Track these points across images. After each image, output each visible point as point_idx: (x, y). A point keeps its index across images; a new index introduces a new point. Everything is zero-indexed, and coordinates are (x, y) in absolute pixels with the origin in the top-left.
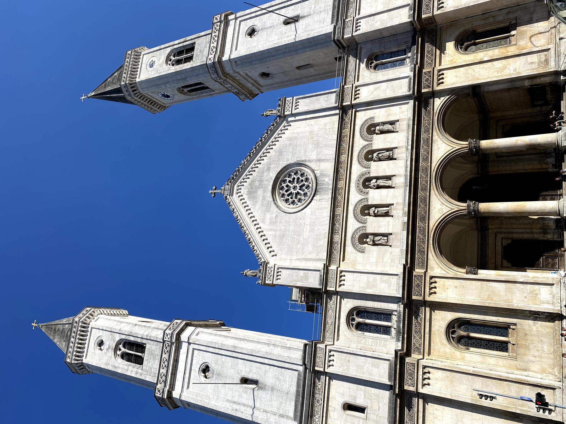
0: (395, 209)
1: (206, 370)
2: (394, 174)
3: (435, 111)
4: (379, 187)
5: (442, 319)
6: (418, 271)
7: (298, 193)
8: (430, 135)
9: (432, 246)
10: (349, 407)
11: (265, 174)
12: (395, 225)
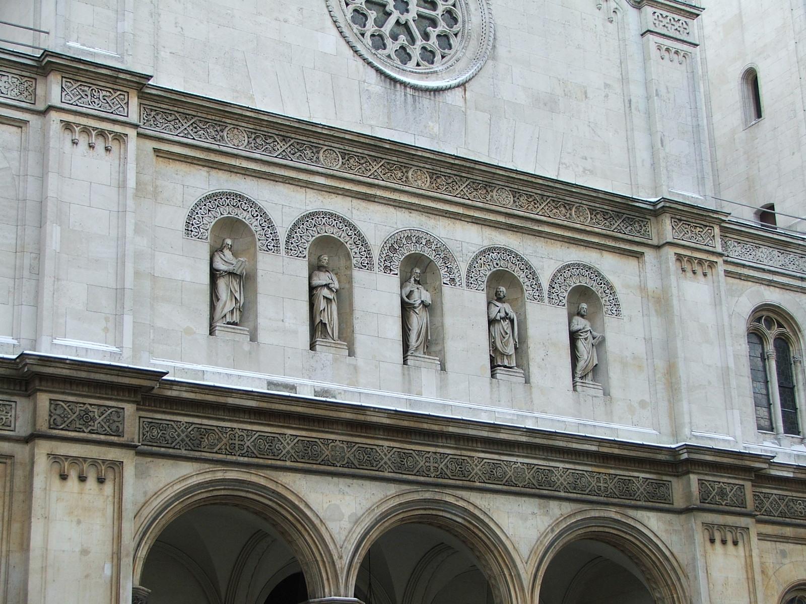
0: (335, 360)
2: (448, 366)
3: (631, 512)
4: (406, 308)
8: (562, 494)
9: (219, 475)
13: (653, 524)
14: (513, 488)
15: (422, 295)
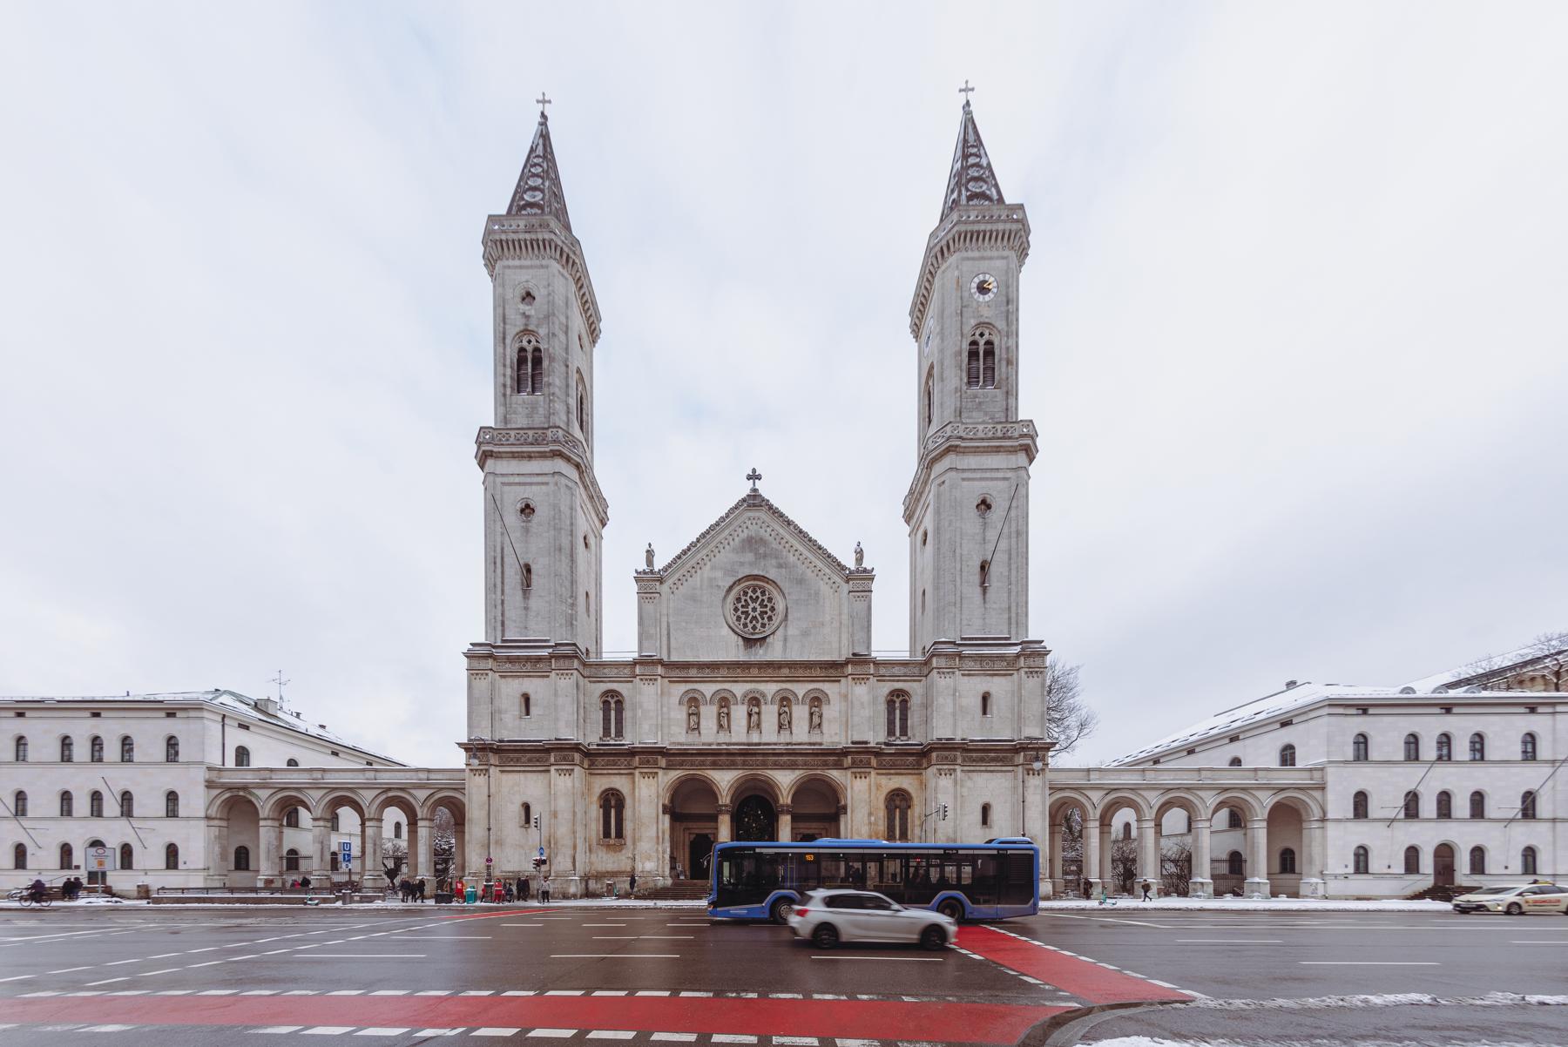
1: (527, 510)
4: (750, 715)
5: (620, 783)
6: (663, 762)
7: (746, 613)
10: (527, 699)
11: (774, 562)
12: (709, 734)
13: (835, 774)
14: (783, 767)
15: (756, 709)
